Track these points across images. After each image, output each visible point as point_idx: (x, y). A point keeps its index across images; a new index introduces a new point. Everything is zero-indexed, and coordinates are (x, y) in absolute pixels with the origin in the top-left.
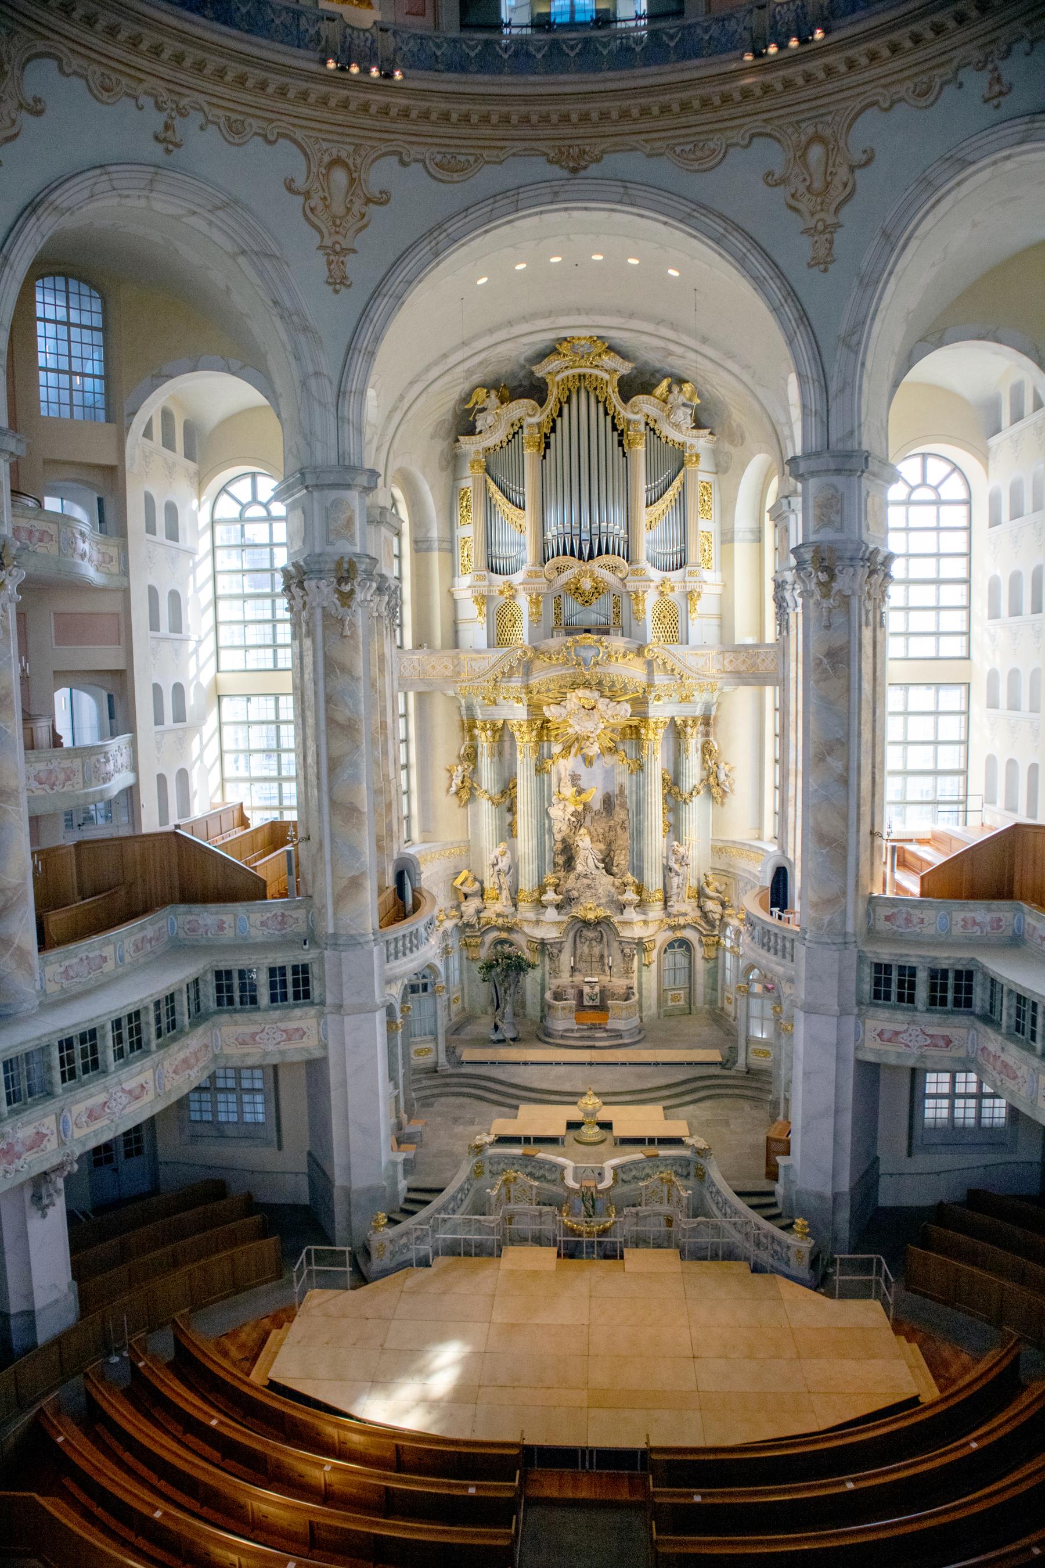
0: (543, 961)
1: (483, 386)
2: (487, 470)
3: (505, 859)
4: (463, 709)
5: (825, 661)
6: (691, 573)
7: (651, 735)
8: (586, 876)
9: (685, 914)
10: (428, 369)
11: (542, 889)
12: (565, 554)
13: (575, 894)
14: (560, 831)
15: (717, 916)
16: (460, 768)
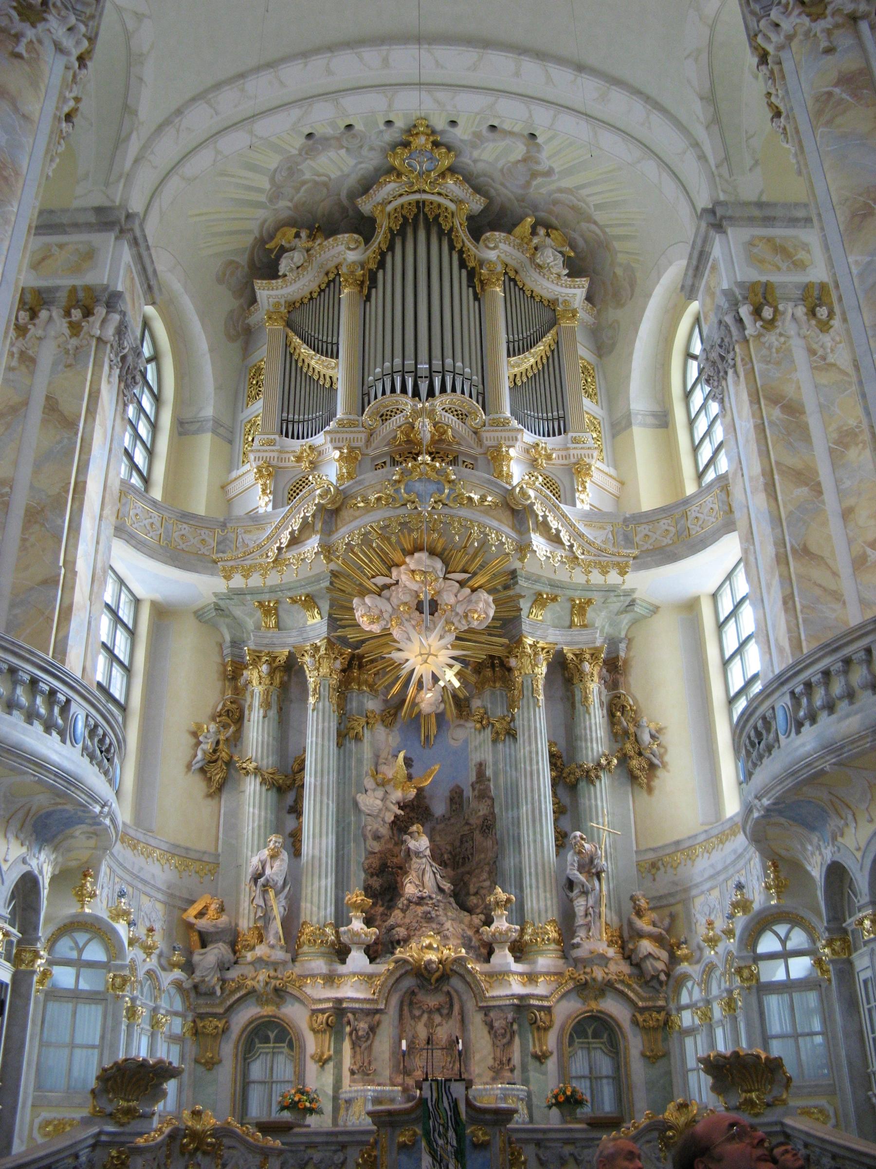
0: (339, 1051)
1: (293, 226)
2: (289, 324)
3: (277, 863)
4: (228, 644)
5: (837, 90)
6: (575, 441)
7: (528, 670)
8: (421, 901)
9: (603, 959)
10: (218, 86)
11: (341, 919)
12: (393, 390)
13: (401, 932)
14: (377, 837)
15: (660, 966)
16: (213, 727)
